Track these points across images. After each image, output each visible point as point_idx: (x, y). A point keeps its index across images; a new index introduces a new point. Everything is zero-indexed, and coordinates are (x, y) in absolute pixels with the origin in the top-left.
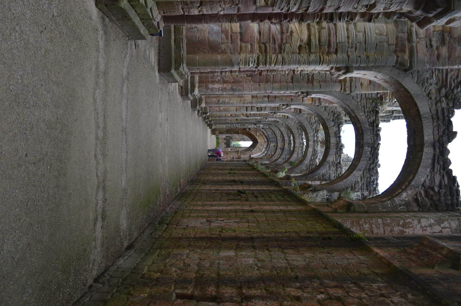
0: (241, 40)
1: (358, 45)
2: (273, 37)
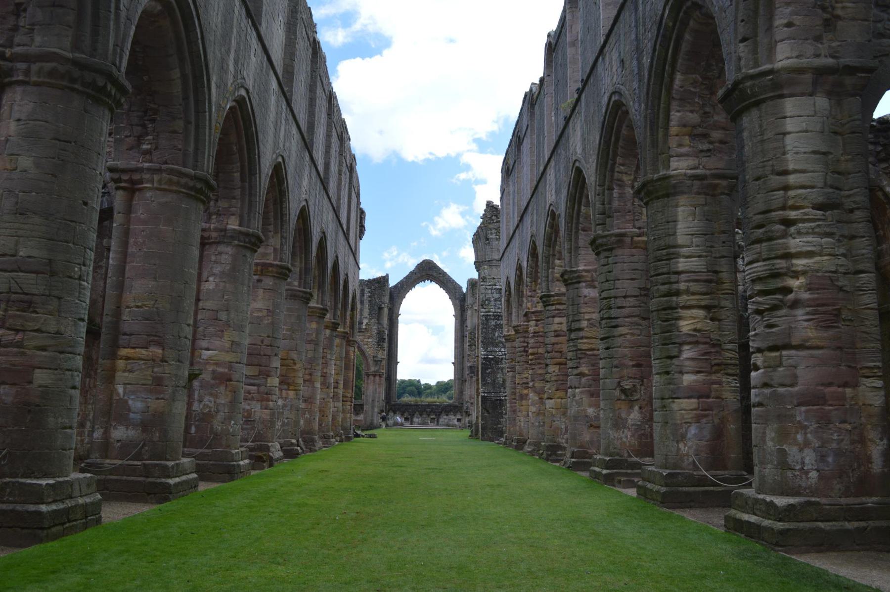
0: (708, 397)
1: (708, 244)
2: (703, 355)
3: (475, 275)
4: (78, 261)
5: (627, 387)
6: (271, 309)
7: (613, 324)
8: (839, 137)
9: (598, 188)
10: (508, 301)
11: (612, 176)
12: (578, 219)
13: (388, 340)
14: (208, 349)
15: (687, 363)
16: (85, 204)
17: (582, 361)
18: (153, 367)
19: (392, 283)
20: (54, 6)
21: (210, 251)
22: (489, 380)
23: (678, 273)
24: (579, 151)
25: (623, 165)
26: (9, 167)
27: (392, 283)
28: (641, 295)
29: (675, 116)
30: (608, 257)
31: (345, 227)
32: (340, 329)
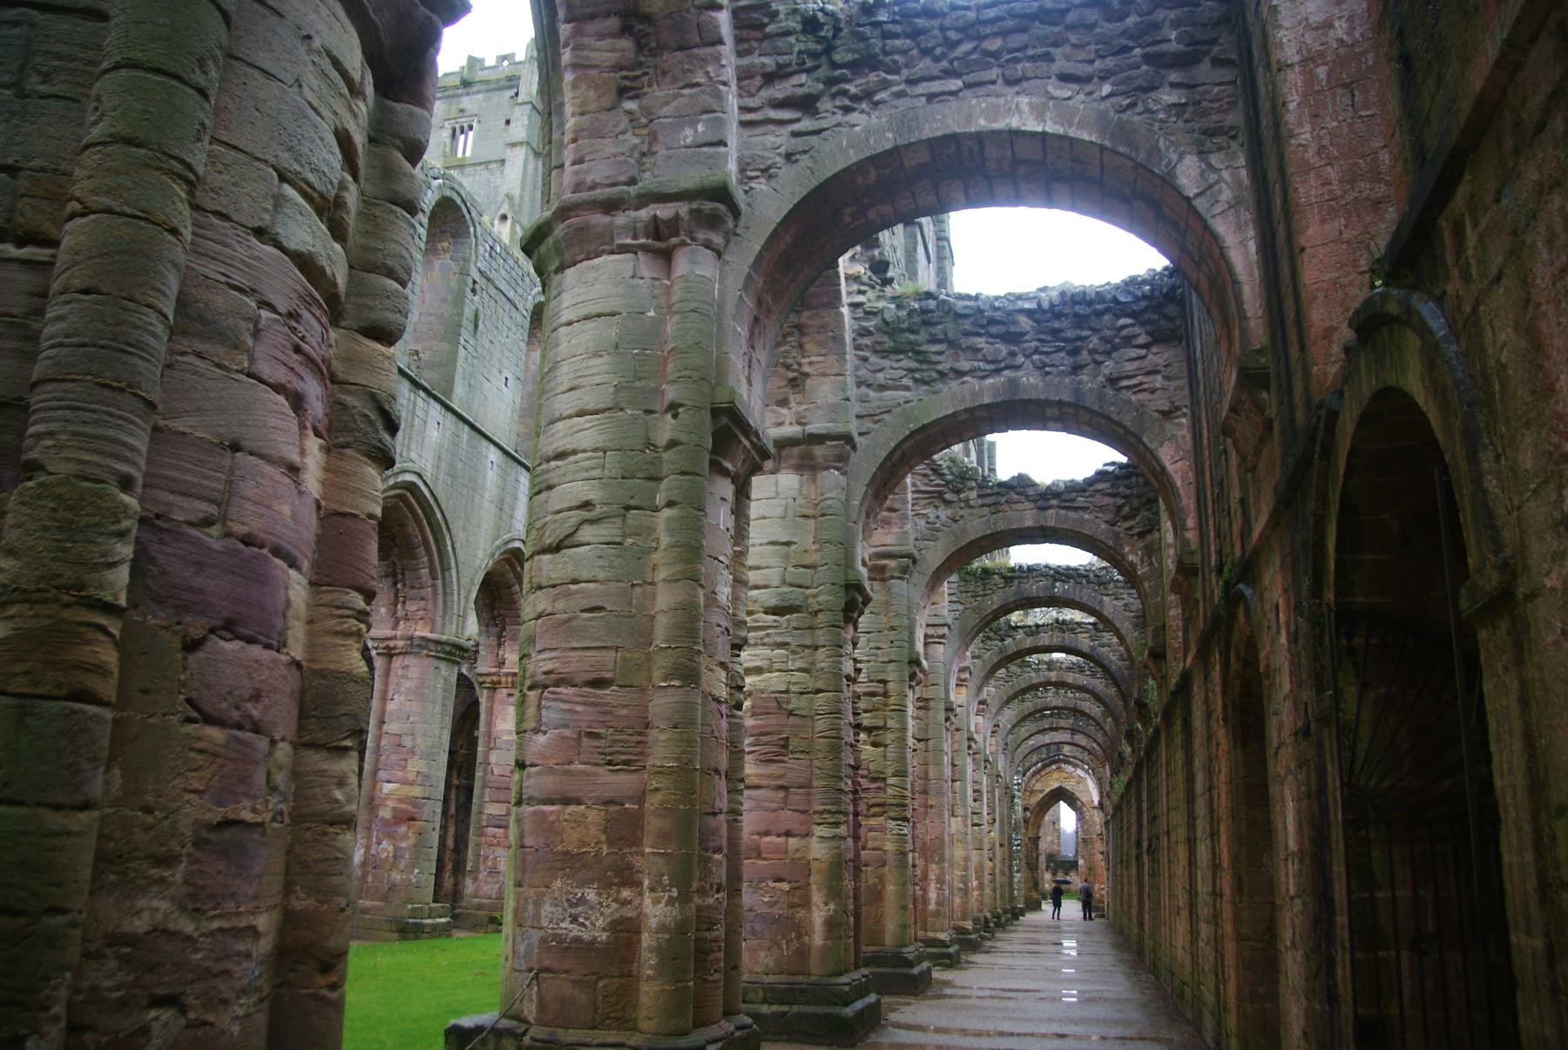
1: (872, 645)
8: (812, 522)
14: (389, 782)
21: (397, 662)
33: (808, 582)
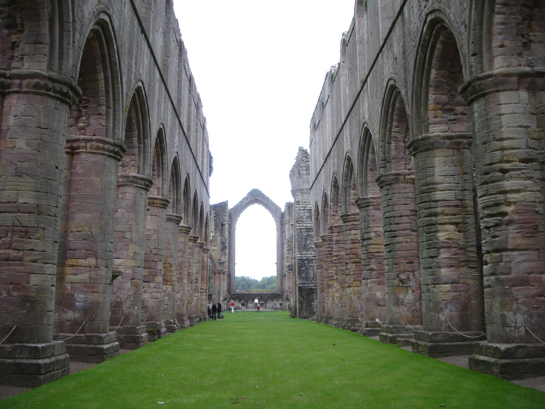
1: (456, 182)
2: (454, 255)
3: (292, 200)
4: (54, 205)
5: (403, 278)
6: (156, 229)
7: (394, 235)
9: (380, 142)
10: (317, 219)
11: (390, 134)
12: (367, 163)
13: (228, 247)
14: (118, 258)
15: (443, 261)
16: (57, 168)
17: (372, 260)
18: (90, 271)
19: (230, 206)
20: (36, 43)
22: (303, 275)
23: (436, 201)
24: (367, 117)
25: (397, 127)
26: (10, 146)
27: (230, 206)
28: (412, 215)
29: (432, 97)
30: (388, 190)
31: (200, 168)
32: (199, 241)
33: (536, 147)
